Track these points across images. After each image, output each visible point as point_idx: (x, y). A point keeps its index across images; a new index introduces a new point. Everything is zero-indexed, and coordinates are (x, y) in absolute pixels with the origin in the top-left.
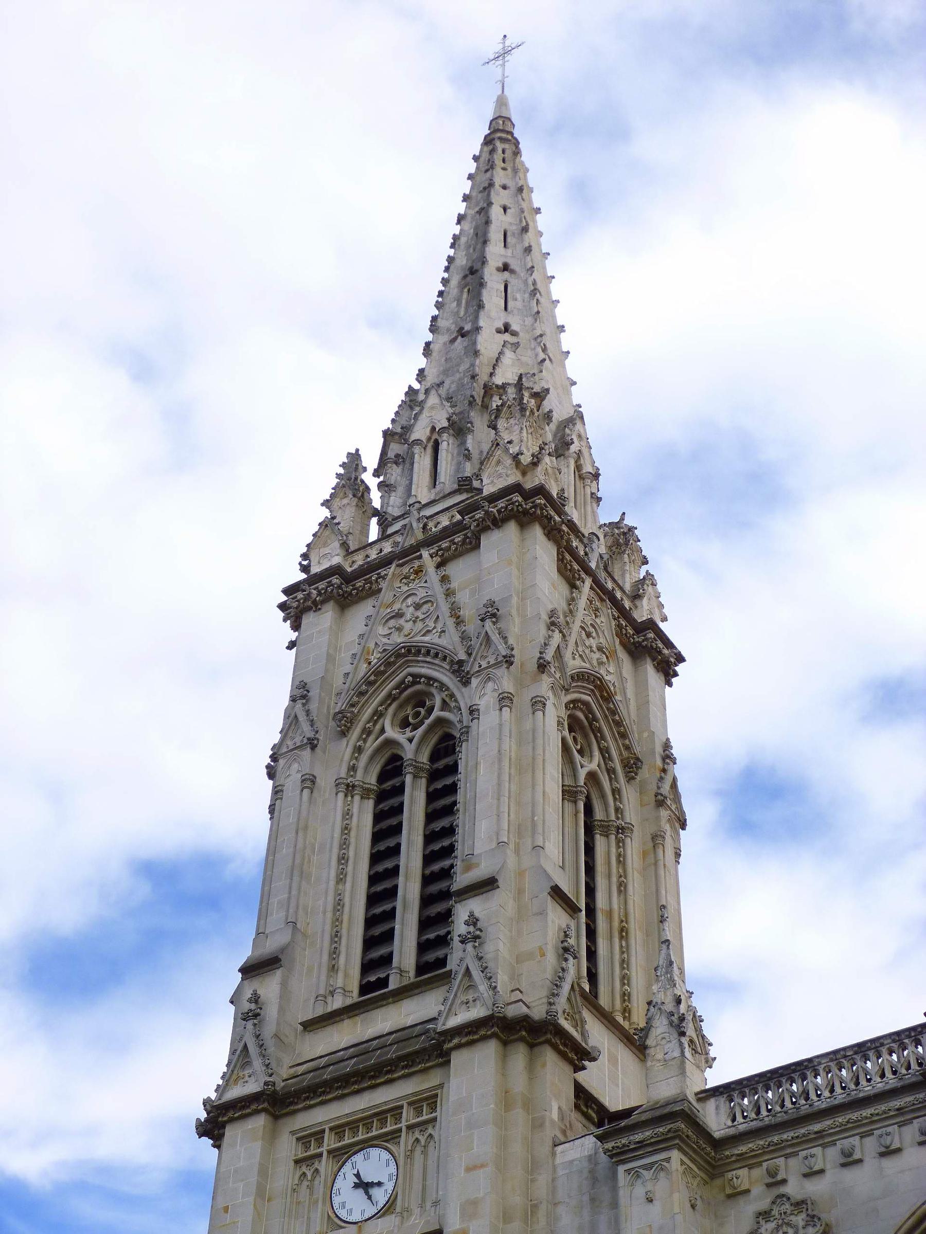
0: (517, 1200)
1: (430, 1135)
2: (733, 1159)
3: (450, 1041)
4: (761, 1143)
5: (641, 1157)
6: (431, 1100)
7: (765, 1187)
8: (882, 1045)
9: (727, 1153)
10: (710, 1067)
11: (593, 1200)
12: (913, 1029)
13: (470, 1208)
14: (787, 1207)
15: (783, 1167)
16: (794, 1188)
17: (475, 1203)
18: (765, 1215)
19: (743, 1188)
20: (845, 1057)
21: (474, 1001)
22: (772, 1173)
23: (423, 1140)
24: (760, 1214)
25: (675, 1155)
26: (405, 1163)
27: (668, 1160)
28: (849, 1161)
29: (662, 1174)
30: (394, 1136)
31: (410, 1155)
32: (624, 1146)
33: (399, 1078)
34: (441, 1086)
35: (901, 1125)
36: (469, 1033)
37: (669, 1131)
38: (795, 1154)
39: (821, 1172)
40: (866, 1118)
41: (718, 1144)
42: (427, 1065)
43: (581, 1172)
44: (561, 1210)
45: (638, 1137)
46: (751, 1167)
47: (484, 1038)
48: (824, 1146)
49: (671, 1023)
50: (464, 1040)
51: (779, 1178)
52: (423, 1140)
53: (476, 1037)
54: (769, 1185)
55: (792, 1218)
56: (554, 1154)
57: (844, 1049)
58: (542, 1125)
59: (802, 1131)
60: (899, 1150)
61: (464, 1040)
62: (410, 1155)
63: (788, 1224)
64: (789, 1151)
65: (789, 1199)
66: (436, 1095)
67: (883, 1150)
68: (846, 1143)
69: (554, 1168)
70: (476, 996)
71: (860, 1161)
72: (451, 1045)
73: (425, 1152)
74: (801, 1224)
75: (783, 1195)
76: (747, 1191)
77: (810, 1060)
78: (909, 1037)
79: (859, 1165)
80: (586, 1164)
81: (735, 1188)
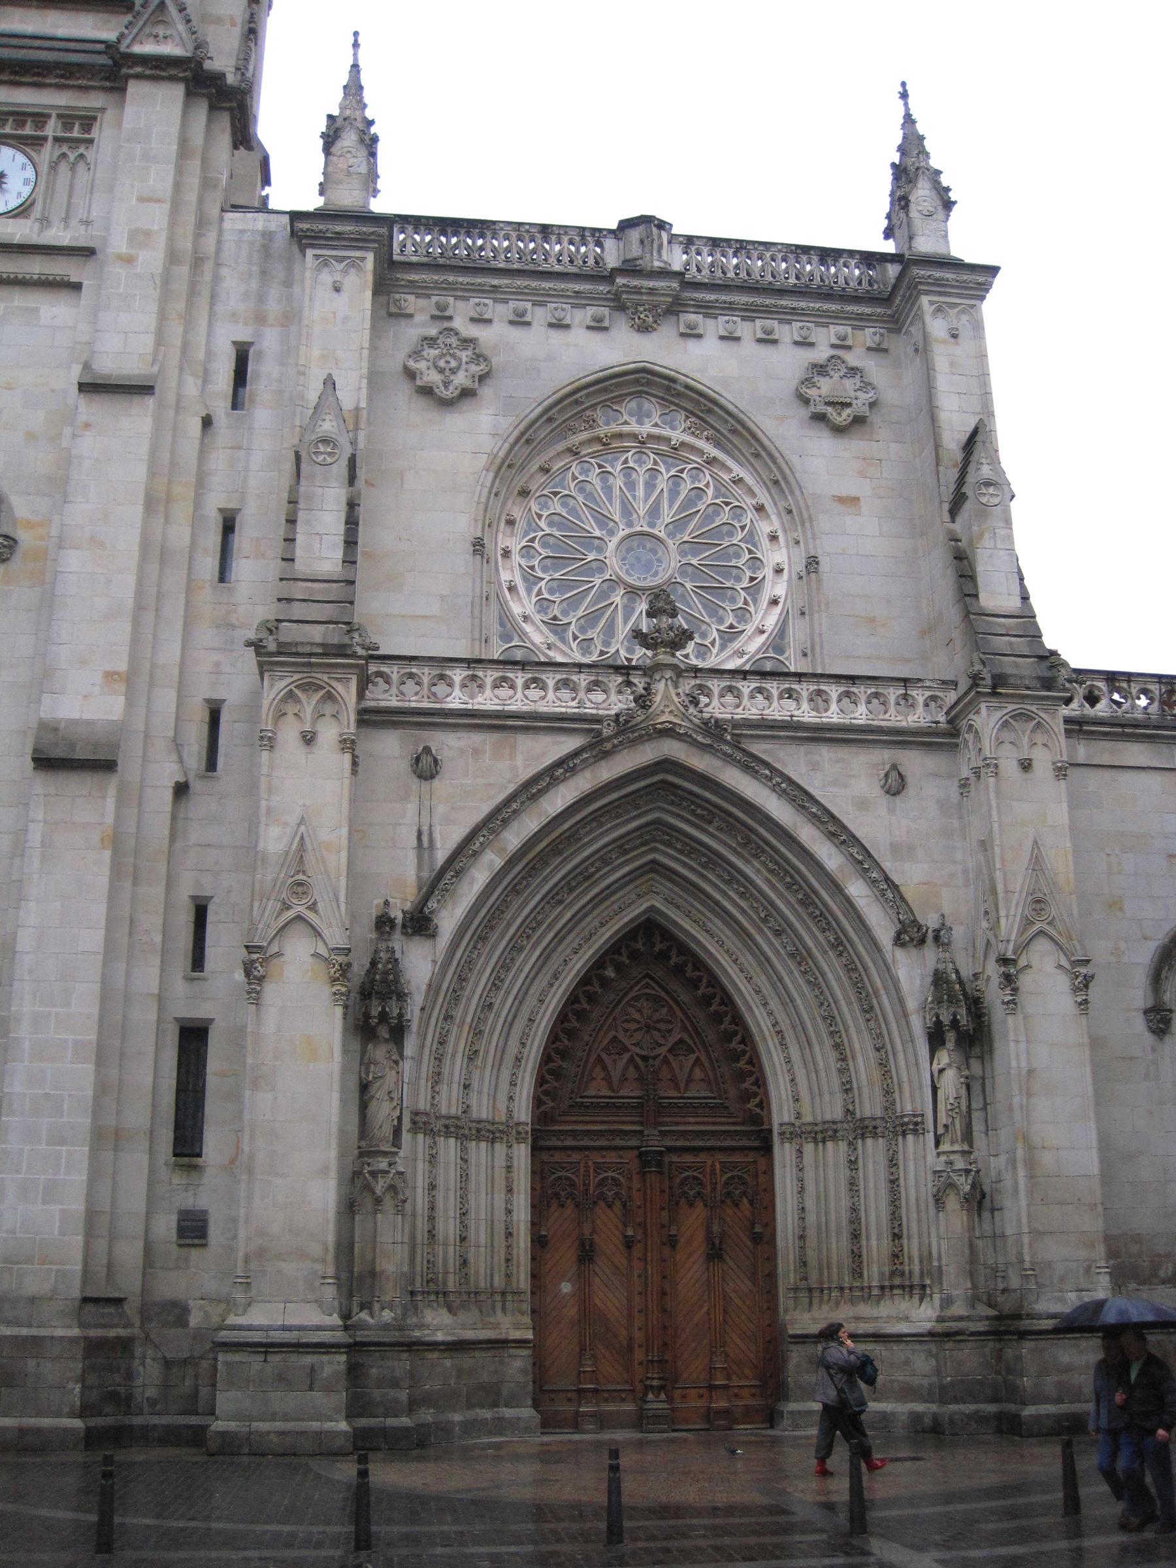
0: (186, 245)
1: (82, 156)
2: (403, 283)
3: (130, 67)
4: (436, 278)
5: (334, 248)
6: (88, 121)
7: (428, 317)
8: (566, 233)
9: (398, 276)
10: (375, 197)
11: (263, 273)
12: (600, 230)
13: (140, 237)
14: (453, 341)
15: (451, 305)
16: (459, 323)
17: (148, 234)
18: (431, 341)
19: (408, 311)
20: (528, 231)
21: (165, 38)
22: (442, 307)
23: (72, 157)
24: (426, 338)
25: (370, 257)
26: (49, 174)
27: (363, 259)
28: (520, 321)
29: (353, 271)
30: (37, 142)
31: (54, 167)
32: (320, 231)
33: (50, 85)
34: (103, 110)
35: (574, 306)
36: (156, 67)
37: (373, 233)
38: (466, 299)
39: (489, 321)
40: (544, 289)
41: (393, 264)
42: (91, 83)
43: (252, 243)
44: (224, 271)
45: (339, 228)
46: (418, 296)
47: (172, 79)
48: (495, 300)
49: (362, 141)
50: (148, 72)
51: (447, 314)
52: (72, 157)
53: (163, 74)
54: (433, 317)
55: (458, 353)
56: (222, 219)
57: (530, 224)
58: (215, 186)
59: (479, 280)
60: (567, 327)
61: (148, 72)
62: (54, 167)
63: (453, 356)
64: (459, 294)
65: (457, 334)
66: (95, 118)
67: (554, 321)
68: (521, 305)
69: (221, 231)
70: (168, 32)
71: (528, 324)
72: (131, 72)
73: (73, 169)
74: (464, 359)
75: (452, 330)
76: (411, 316)
77: (494, 223)
78: (593, 236)
79: (526, 328)
80: (259, 238)
81: (400, 308)
